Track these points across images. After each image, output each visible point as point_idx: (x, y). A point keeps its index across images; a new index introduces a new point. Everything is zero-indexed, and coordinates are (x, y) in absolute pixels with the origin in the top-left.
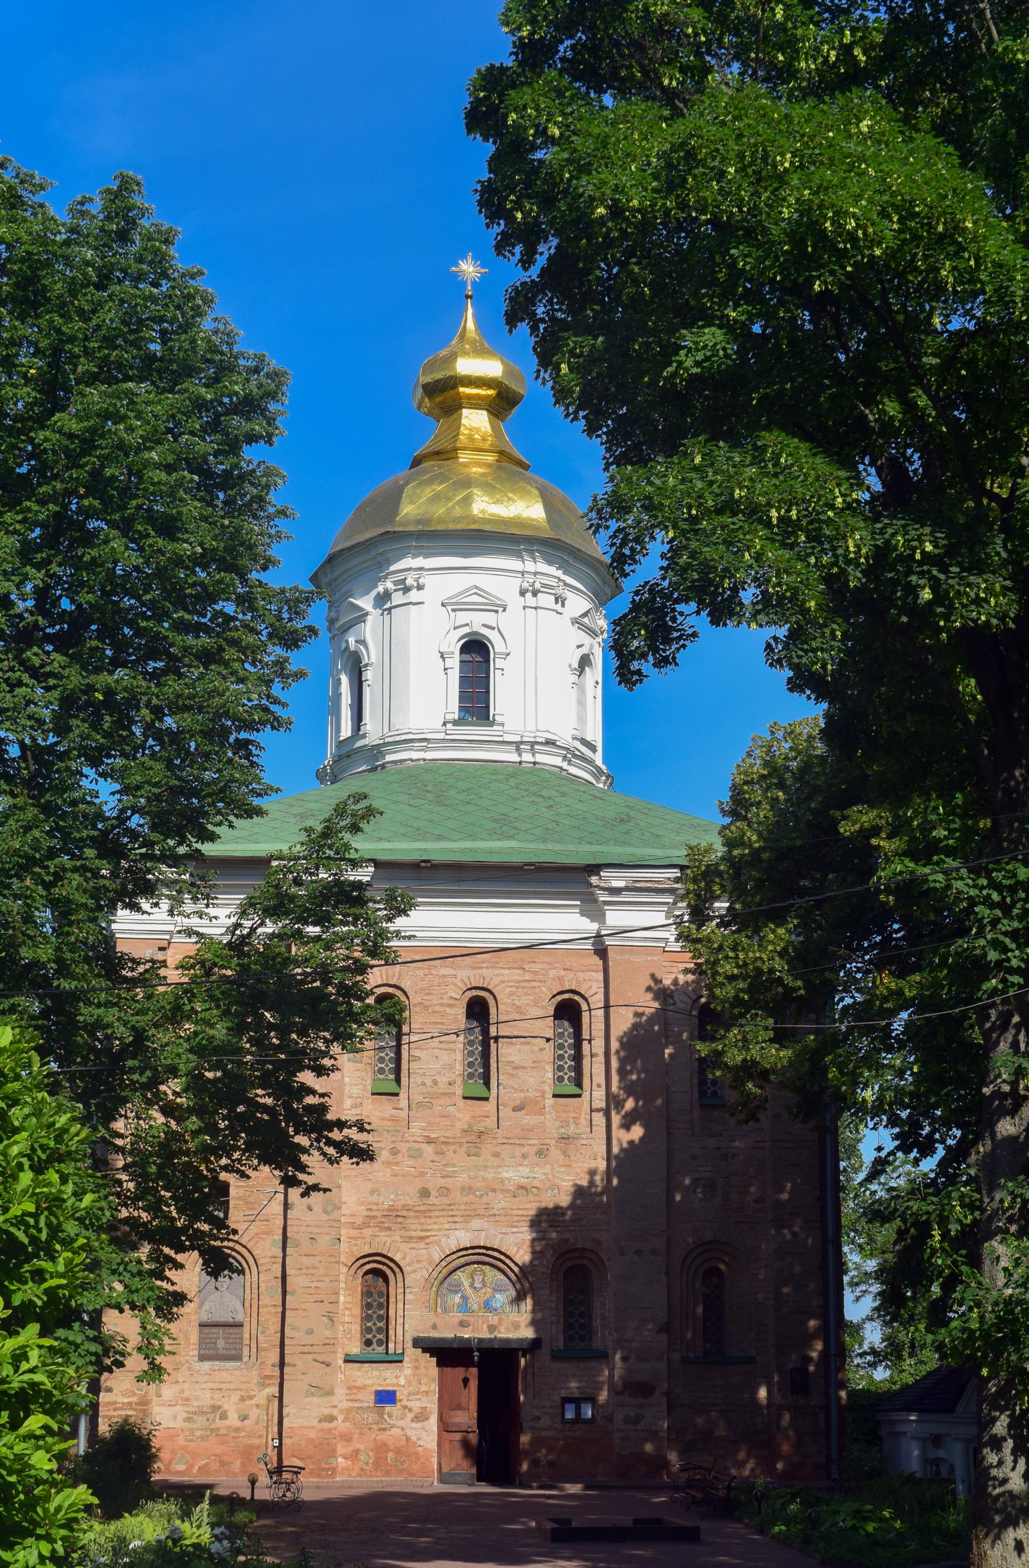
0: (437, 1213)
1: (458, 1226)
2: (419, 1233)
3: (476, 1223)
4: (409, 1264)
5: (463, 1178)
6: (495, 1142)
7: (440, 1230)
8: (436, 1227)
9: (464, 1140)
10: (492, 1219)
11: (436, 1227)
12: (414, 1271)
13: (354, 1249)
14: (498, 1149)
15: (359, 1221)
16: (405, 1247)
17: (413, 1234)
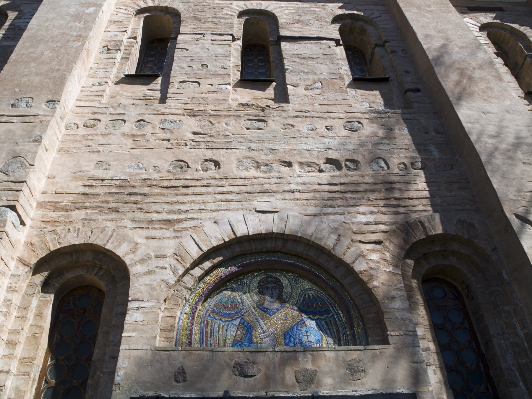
0: (198, 190)
1: (233, 205)
2: (165, 216)
3: (262, 203)
4: (142, 261)
5: (241, 151)
6: (284, 114)
7: (201, 210)
8: (196, 207)
9: (241, 113)
10: (287, 196)
11: (196, 207)
12: (150, 272)
13: (49, 237)
14: (290, 121)
15: (66, 200)
16: (139, 236)
17: (155, 216)
